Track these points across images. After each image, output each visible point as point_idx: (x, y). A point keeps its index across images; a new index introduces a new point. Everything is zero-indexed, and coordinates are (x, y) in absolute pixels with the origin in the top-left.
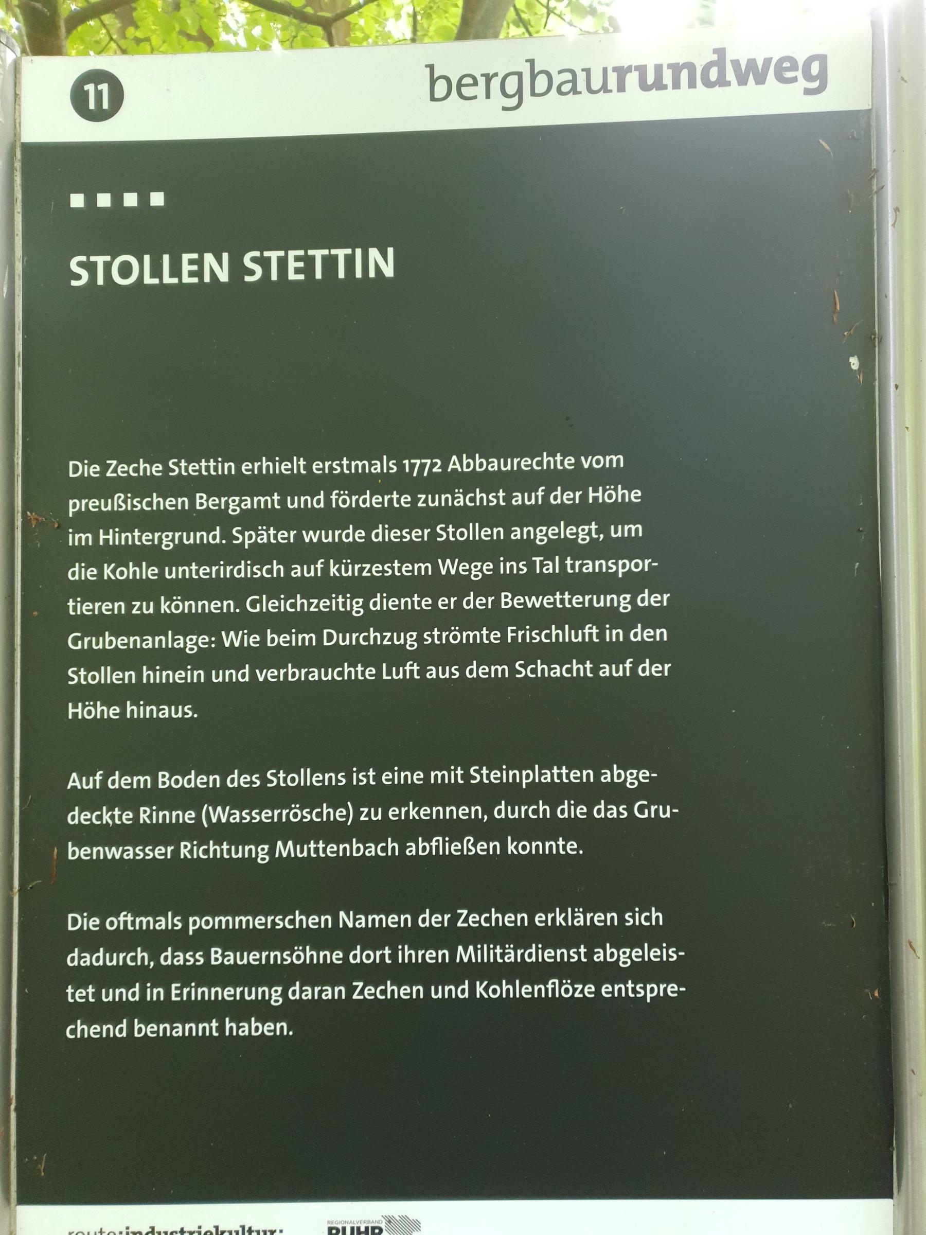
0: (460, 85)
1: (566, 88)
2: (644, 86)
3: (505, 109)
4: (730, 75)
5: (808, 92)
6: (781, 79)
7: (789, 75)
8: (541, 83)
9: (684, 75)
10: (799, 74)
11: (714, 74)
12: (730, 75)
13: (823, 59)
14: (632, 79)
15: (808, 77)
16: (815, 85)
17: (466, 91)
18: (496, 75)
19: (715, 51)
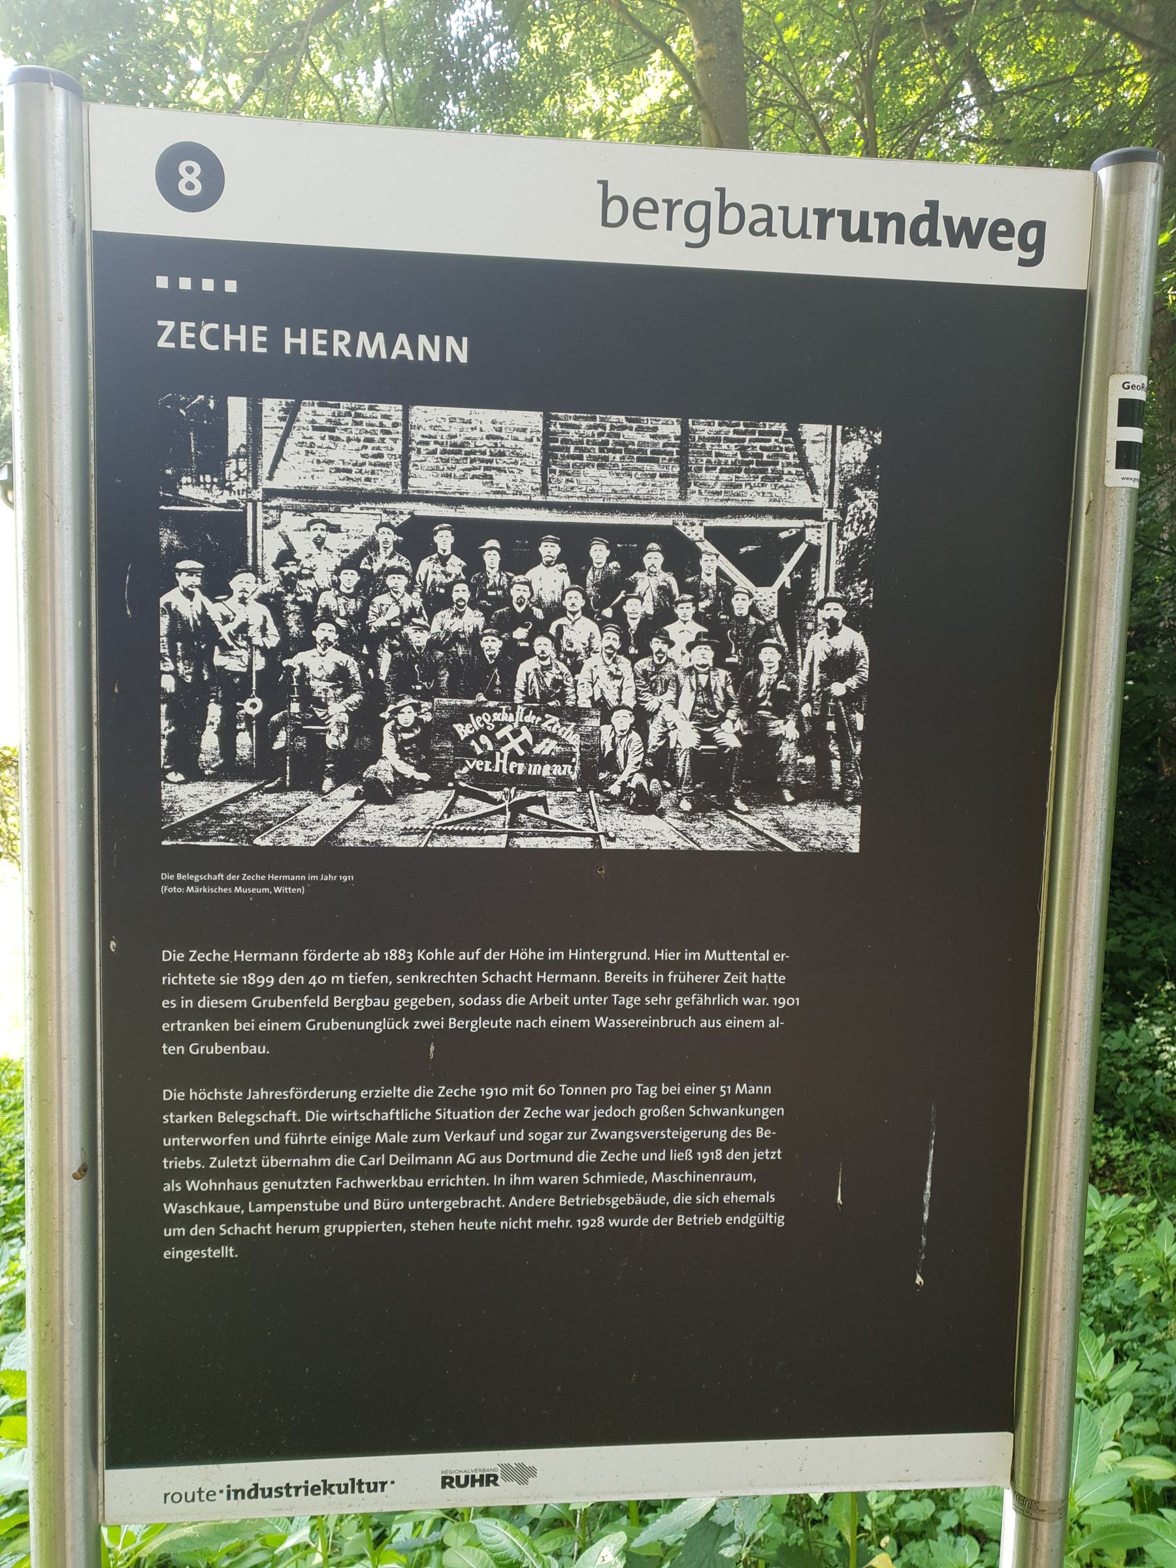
0: (637, 210)
3: (688, 245)
4: (942, 234)
5: (1023, 262)
10: (1014, 241)
12: (942, 234)
14: (834, 225)
15: (1025, 247)
16: (1031, 255)
17: (645, 218)
18: (680, 202)
19: (928, 203)
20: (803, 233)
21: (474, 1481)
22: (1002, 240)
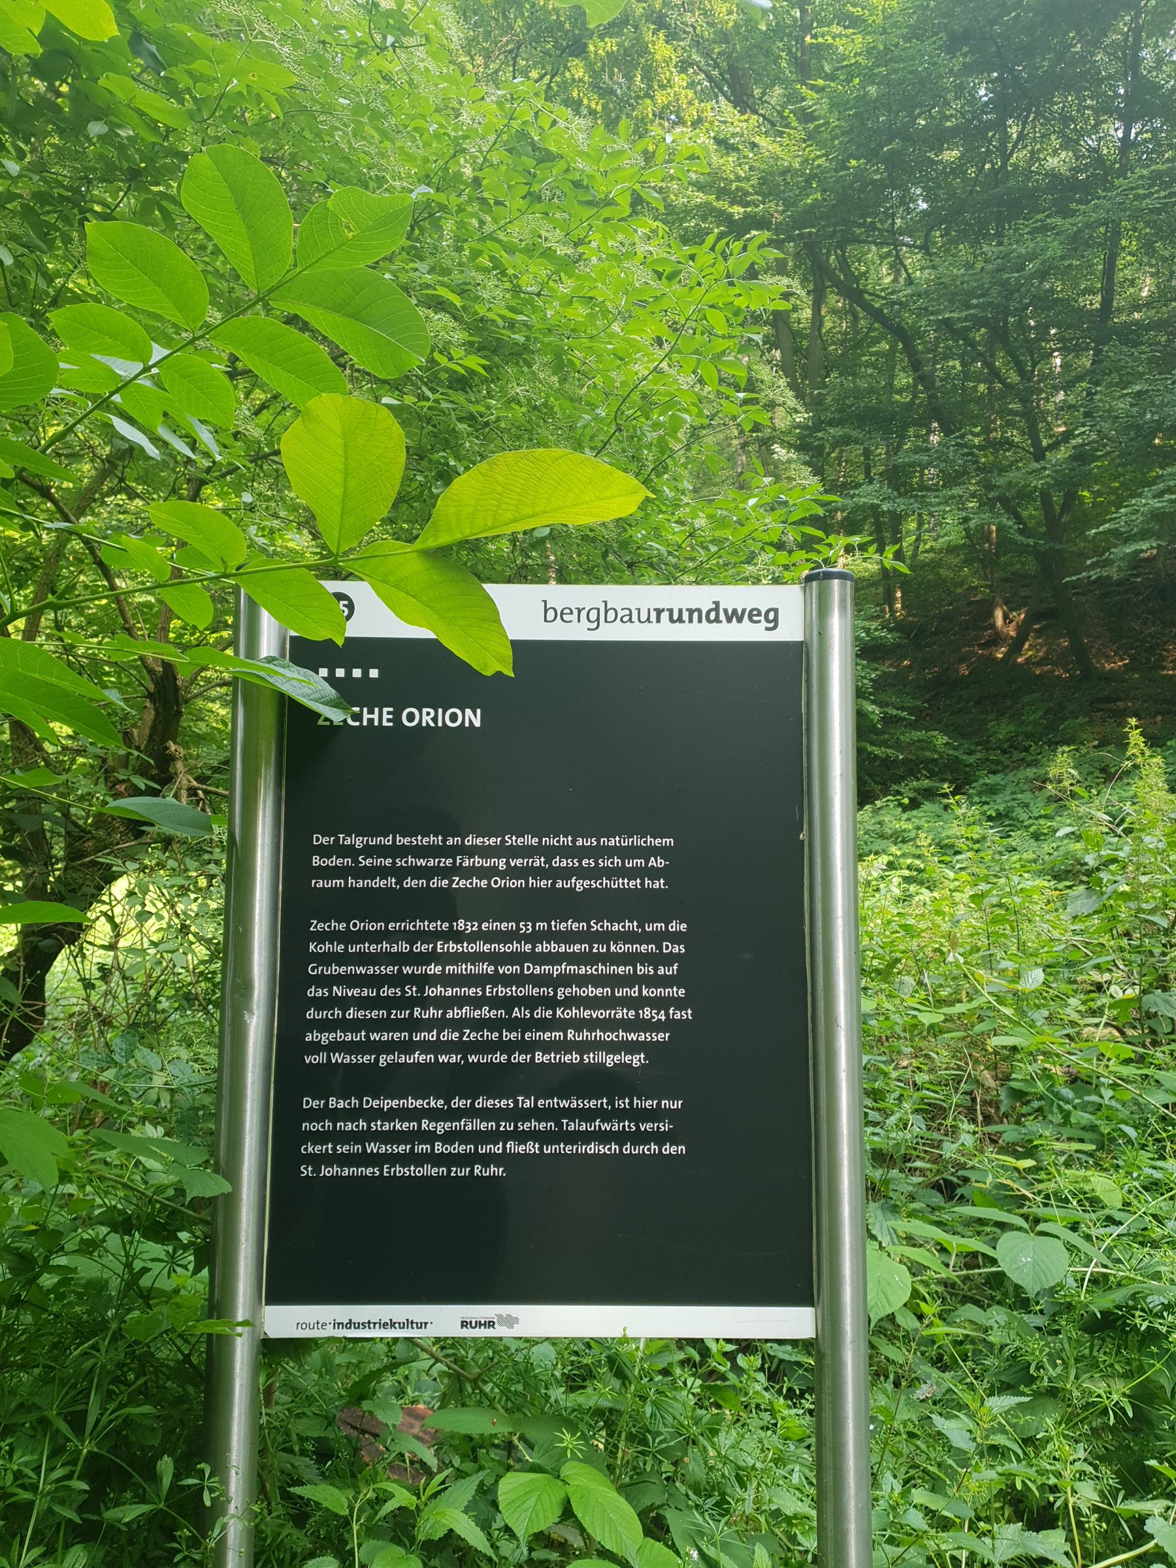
0: (562, 613)
1: (627, 618)
2: (672, 620)
4: (722, 617)
5: (767, 629)
6: (751, 620)
7: (755, 618)
8: (611, 615)
9: (696, 615)
10: (762, 618)
11: (713, 616)
12: (722, 617)
13: (776, 611)
14: (665, 616)
16: (772, 625)
20: (648, 620)
21: (481, 1324)
22: (755, 618)
